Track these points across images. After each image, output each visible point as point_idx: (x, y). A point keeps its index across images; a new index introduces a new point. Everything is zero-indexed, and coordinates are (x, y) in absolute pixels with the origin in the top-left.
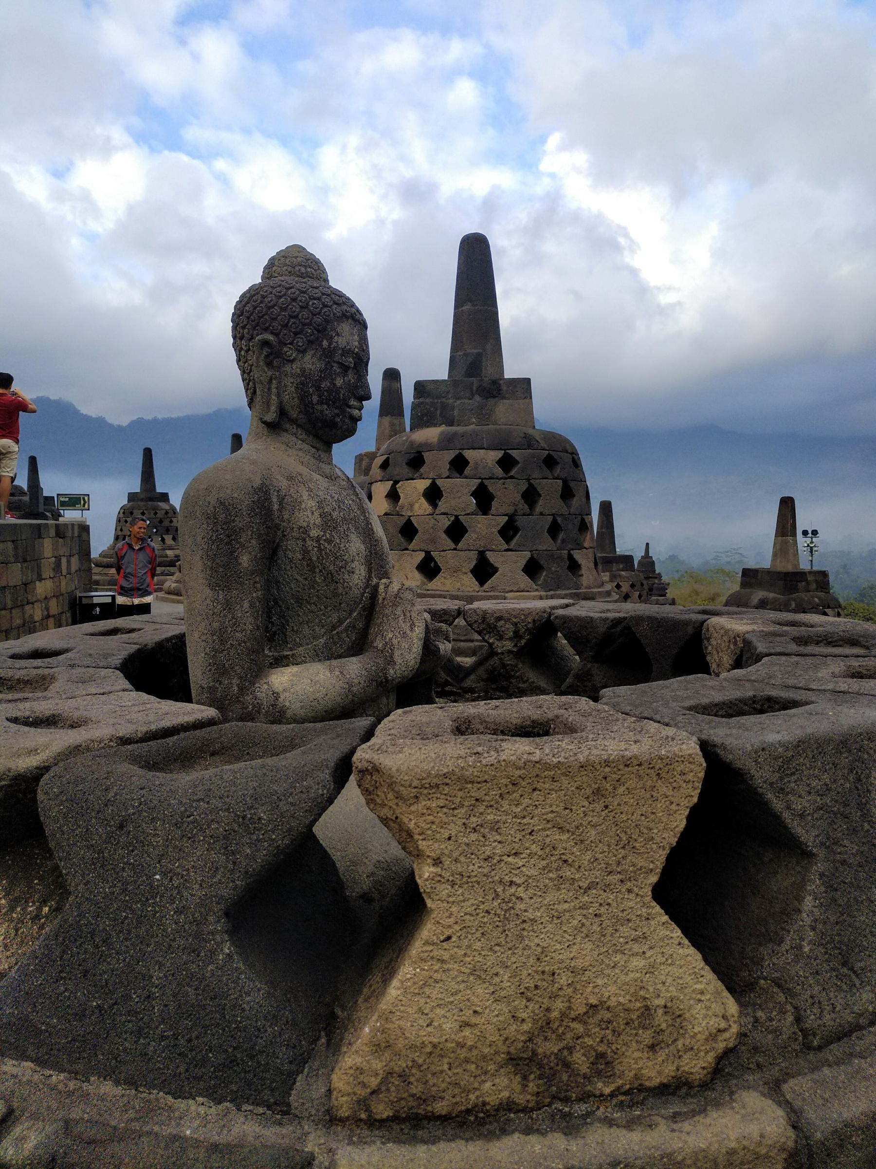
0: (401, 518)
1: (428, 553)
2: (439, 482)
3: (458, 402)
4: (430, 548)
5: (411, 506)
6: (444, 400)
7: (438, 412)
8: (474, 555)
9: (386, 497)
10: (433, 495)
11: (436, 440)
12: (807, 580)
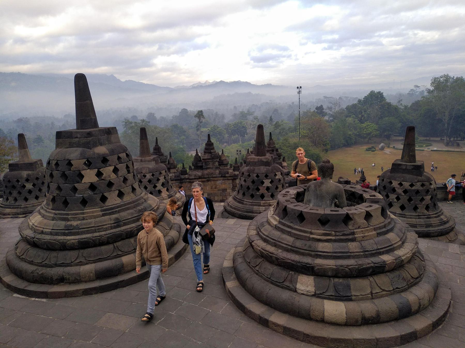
0: (107, 181)
1: (119, 191)
2: (117, 166)
3: (102, 137)
4: (120, 188)
5: (109, 176)
6: (98, 137)
7: (98, 141)
8: (131, 187)
9: (95, 175)
10: (116, 171)
11: (108, 152)
12: (38, 165)
